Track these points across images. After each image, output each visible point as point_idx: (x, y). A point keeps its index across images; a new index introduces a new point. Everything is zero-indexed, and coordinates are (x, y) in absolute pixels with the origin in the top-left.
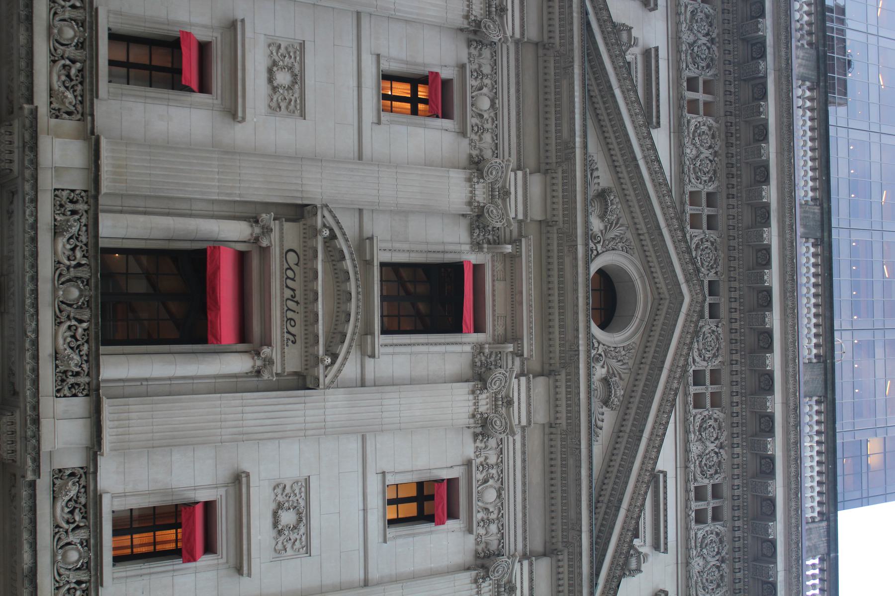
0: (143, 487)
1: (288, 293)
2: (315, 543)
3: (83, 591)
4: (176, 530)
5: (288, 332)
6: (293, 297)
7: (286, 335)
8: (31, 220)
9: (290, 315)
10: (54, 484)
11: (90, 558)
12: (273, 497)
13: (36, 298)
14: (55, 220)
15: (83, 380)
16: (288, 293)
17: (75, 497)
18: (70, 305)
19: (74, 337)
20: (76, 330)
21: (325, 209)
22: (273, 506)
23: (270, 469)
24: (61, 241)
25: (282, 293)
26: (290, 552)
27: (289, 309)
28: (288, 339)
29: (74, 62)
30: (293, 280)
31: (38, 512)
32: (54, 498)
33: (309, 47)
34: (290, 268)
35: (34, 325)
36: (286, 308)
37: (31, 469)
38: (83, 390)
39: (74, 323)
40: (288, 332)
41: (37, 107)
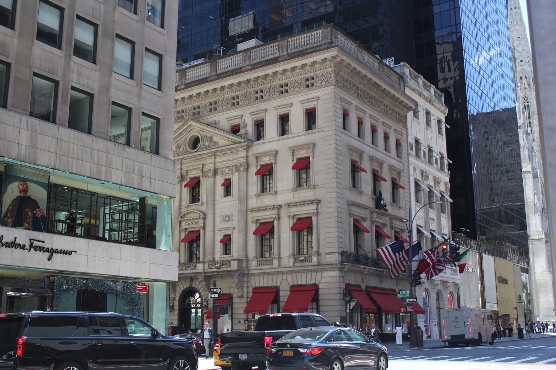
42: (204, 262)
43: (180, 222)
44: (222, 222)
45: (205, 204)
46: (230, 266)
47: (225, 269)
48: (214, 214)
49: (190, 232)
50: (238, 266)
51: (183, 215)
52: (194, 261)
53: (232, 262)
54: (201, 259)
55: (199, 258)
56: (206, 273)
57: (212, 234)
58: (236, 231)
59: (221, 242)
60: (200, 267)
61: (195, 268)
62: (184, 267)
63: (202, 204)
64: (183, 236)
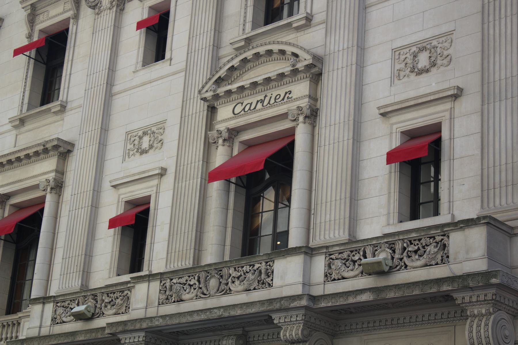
0: (384, 200)
1: (259, 106)
2: (444, 29)
3: (411, 244)
4: (420, 161)
5: (283, 99)
6: (262, 101)
7: (285, 100)
8: (161, 320)
9: (272, 101)
10: (334, 280)
11: (386, 242)
12: (406, 79)
13: (201, 311)
14: (174, 302)
15: (263, 266)
16: (259, 106)
17: (344, 262)
18: (220, 283)
19: (238, 278)
20: (234, 277)
21: (202, 92)
22: (413, 76)
23: (382, 88)
24: (185, 296)
25: (260, 110)
26: (450, 51)
27: (269, 103)
28: (288, 98)
29: (103, 301)
30: (251, 104)
31: (351, 290)
32: (343, 278)
33: (130, 128)
34: (244, 109)
35: (215, 311)
36: (275, 103)
37: (299, 302)
38: (270, 265)
39: (230, 280)
40: (283, 99)
41: (107, 324)
42: (308, 251)
43: (212, 110)
44: (396, 76)
45: (317, 19)
46: (445, 259)
47: (415, 273)
48: (361, 49)
49: (249, 145)
50: (491, 255)
51: (222, 73)
52: (265, 245)
53: (456, 240)
54: (294, 241)
55: (287, 233)
56: (313, 298)
57: (347, 136)
58: (469, 104)
59: (392, 157)
60: (288, 275)
61: (265, 280)
62: (213, 283)
63: (309, 19)
64: (220, 157)
